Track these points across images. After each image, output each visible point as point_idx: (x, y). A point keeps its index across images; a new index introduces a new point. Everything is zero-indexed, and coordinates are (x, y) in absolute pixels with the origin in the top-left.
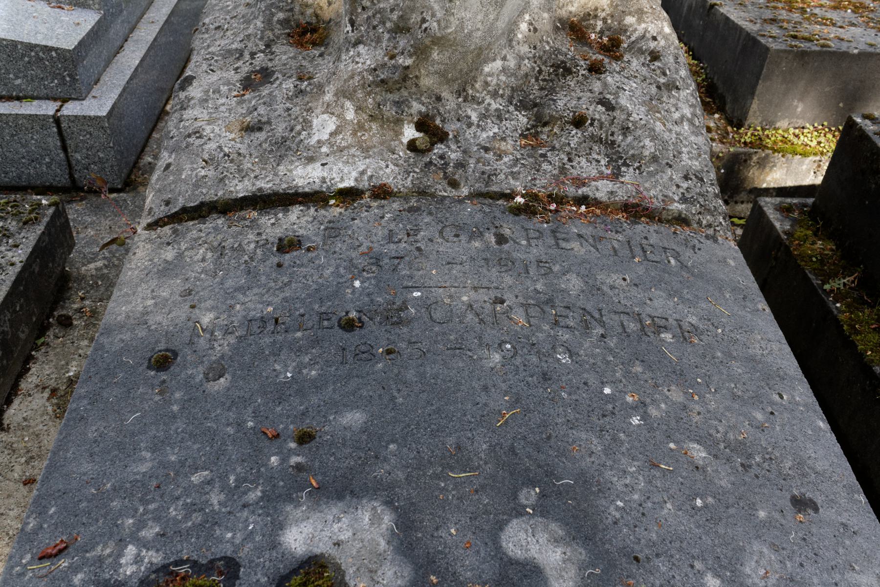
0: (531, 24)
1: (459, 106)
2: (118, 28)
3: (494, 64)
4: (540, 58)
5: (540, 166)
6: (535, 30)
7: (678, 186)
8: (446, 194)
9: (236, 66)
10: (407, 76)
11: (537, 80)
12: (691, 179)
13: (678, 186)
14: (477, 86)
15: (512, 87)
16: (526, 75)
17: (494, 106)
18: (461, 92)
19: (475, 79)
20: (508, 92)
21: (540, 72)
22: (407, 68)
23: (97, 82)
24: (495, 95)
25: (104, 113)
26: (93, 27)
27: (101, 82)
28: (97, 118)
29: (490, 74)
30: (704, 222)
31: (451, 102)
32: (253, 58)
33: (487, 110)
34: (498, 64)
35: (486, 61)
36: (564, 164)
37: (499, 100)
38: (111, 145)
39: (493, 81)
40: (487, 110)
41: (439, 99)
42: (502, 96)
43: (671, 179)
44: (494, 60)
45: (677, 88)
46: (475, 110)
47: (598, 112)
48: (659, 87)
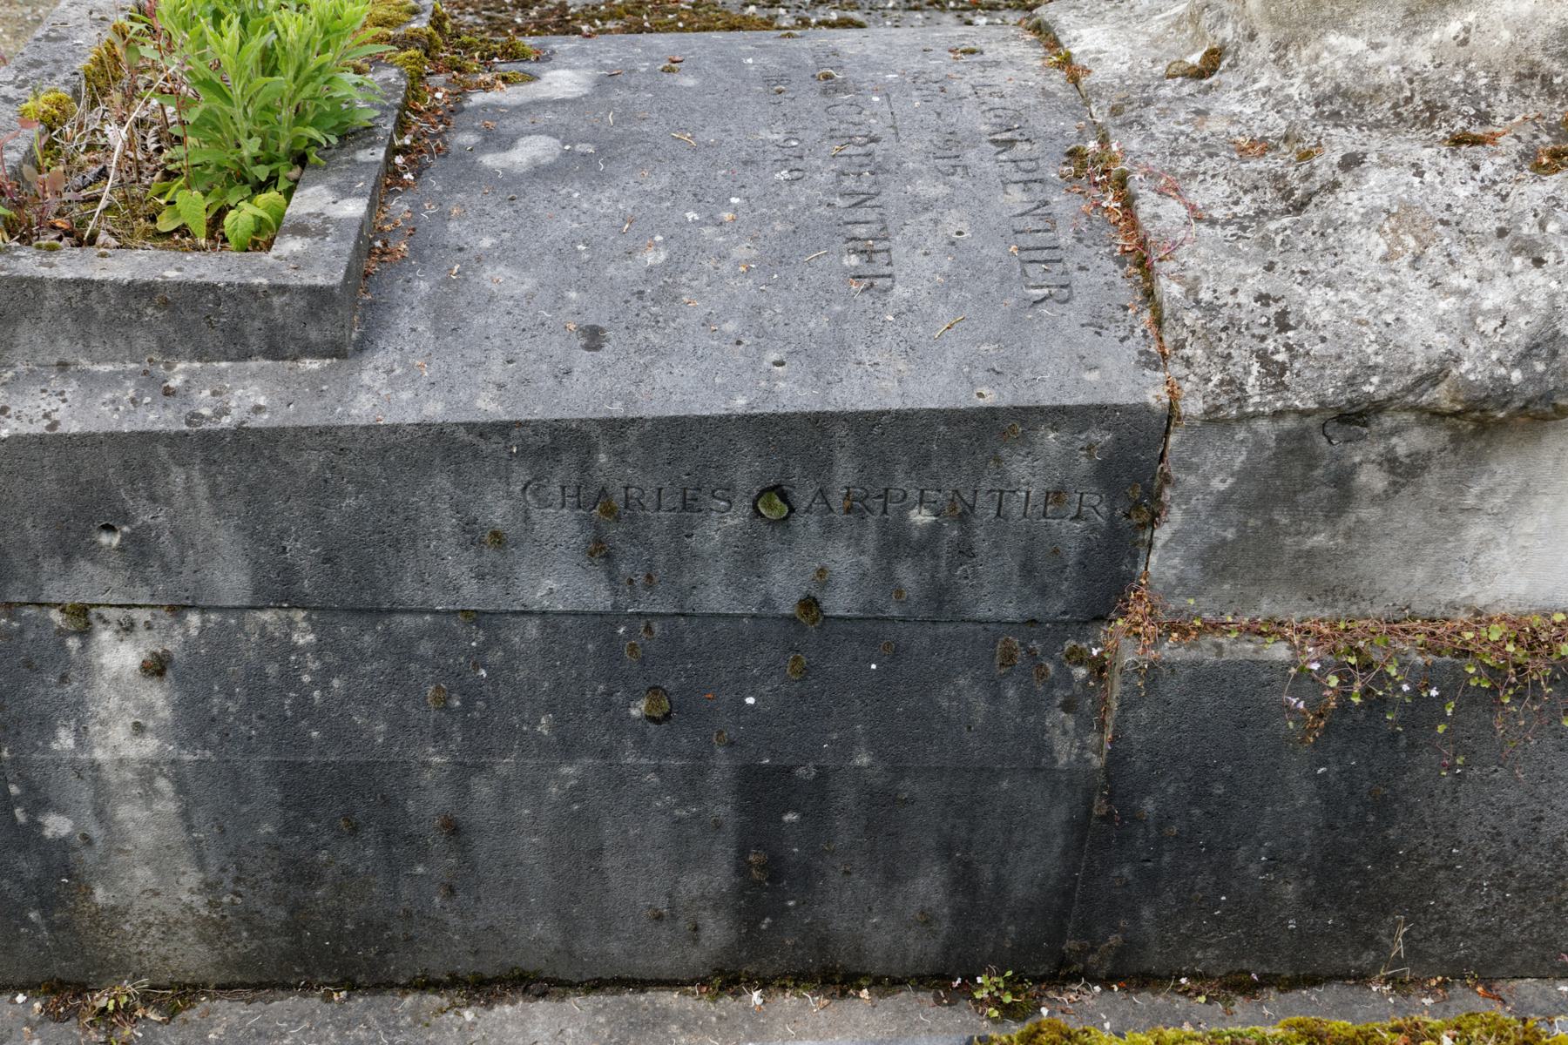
0: (1467, 30)
1: (1264, 62)
3: (1351, 41)
4: (1425, 81)
6: (1465, 42)
7: (1234, 292)
11: (1395, 106)
13: (1234, 292)
14: (1305, 53)
15: (1338, 86)
16: (1379, 88)
17: (1293, 91)
18: (1281, 47)
19: (1306, 41)
20: (1327, 87)
21: (1408, 100)
24: (1309, 77)
29: (1331, 50)
30: (1188, 351)
31: (1261, 50)
33: (1282, 88)
34: (1357, 45)
35: (1339, 25)
37: (1307, 86)
39: (1326, 58)
40: (1282, 88)
41: (1252, 37)
42: (1313, 85)
43: (1242, 278)
44: (1355, 36)
45: (1538, 262)
46: (1272, 78)
48: (1502, 233)
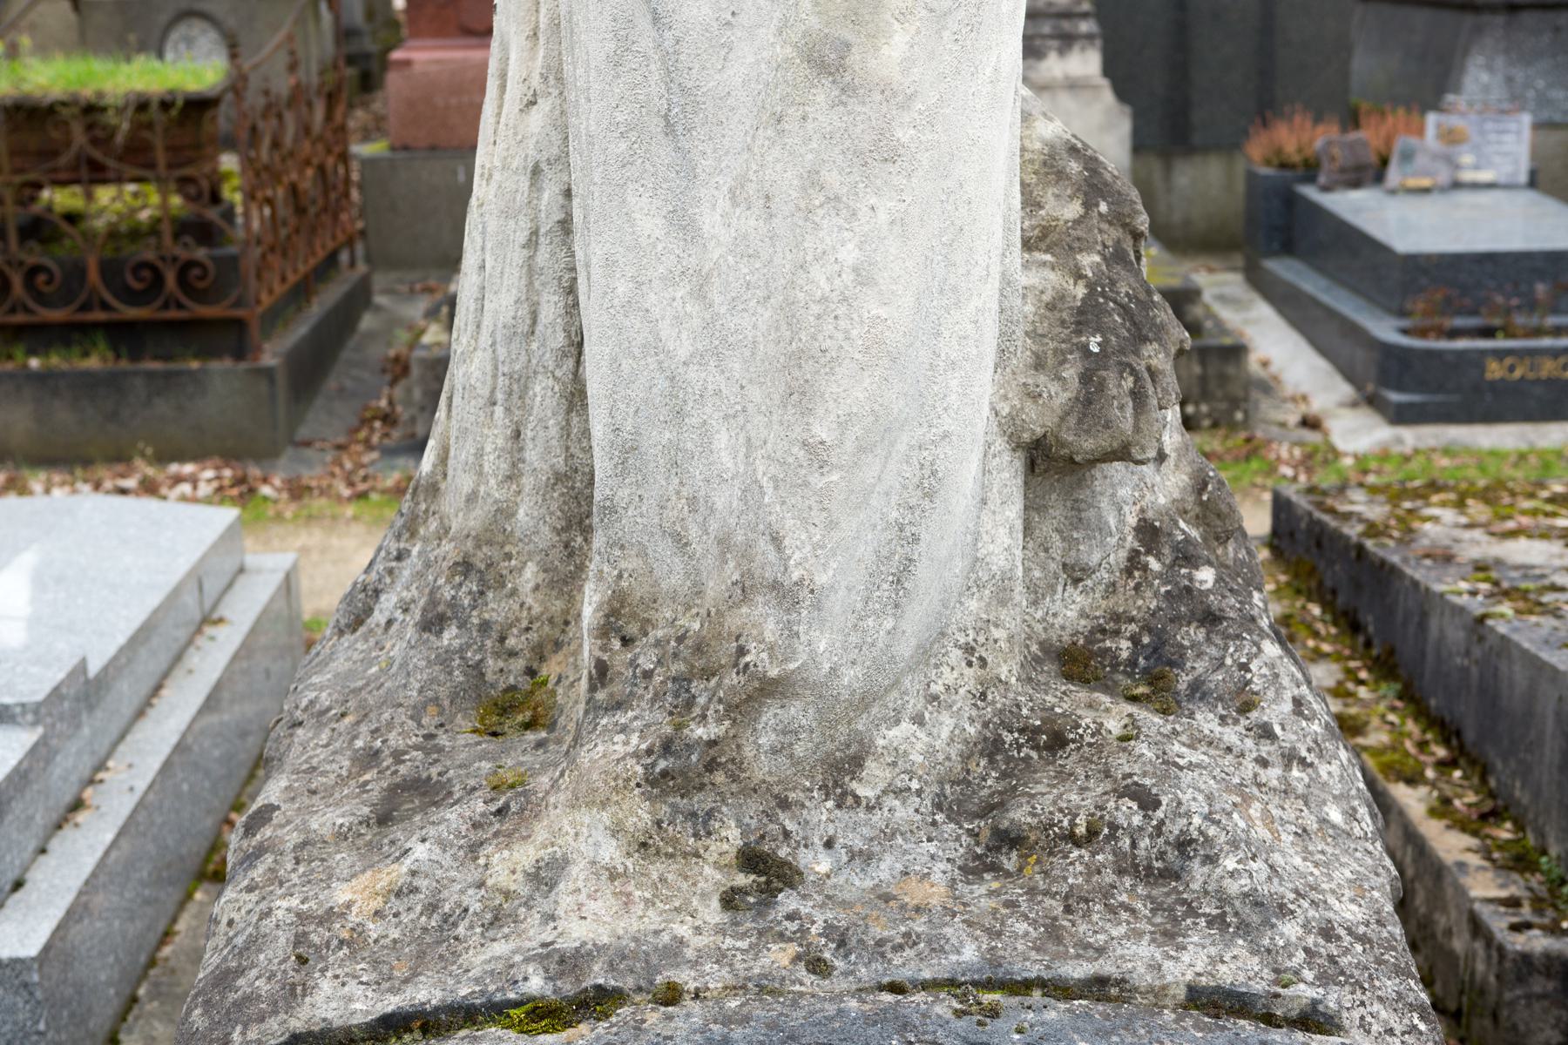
2: (69, 764)
5: (1003, 924)
8: (803, 989)
9: (362, 780)
10: (714, 759)
12: (1339, 938)
22: (712, 743)
23: (18, 885)
25: (31, 949)
26: (20, 763)
27: (27, 886)
28: (15, 962)
32: (399, 762)
36: (1055, 919)
38: (42, 1027)
47: (1127, 813)
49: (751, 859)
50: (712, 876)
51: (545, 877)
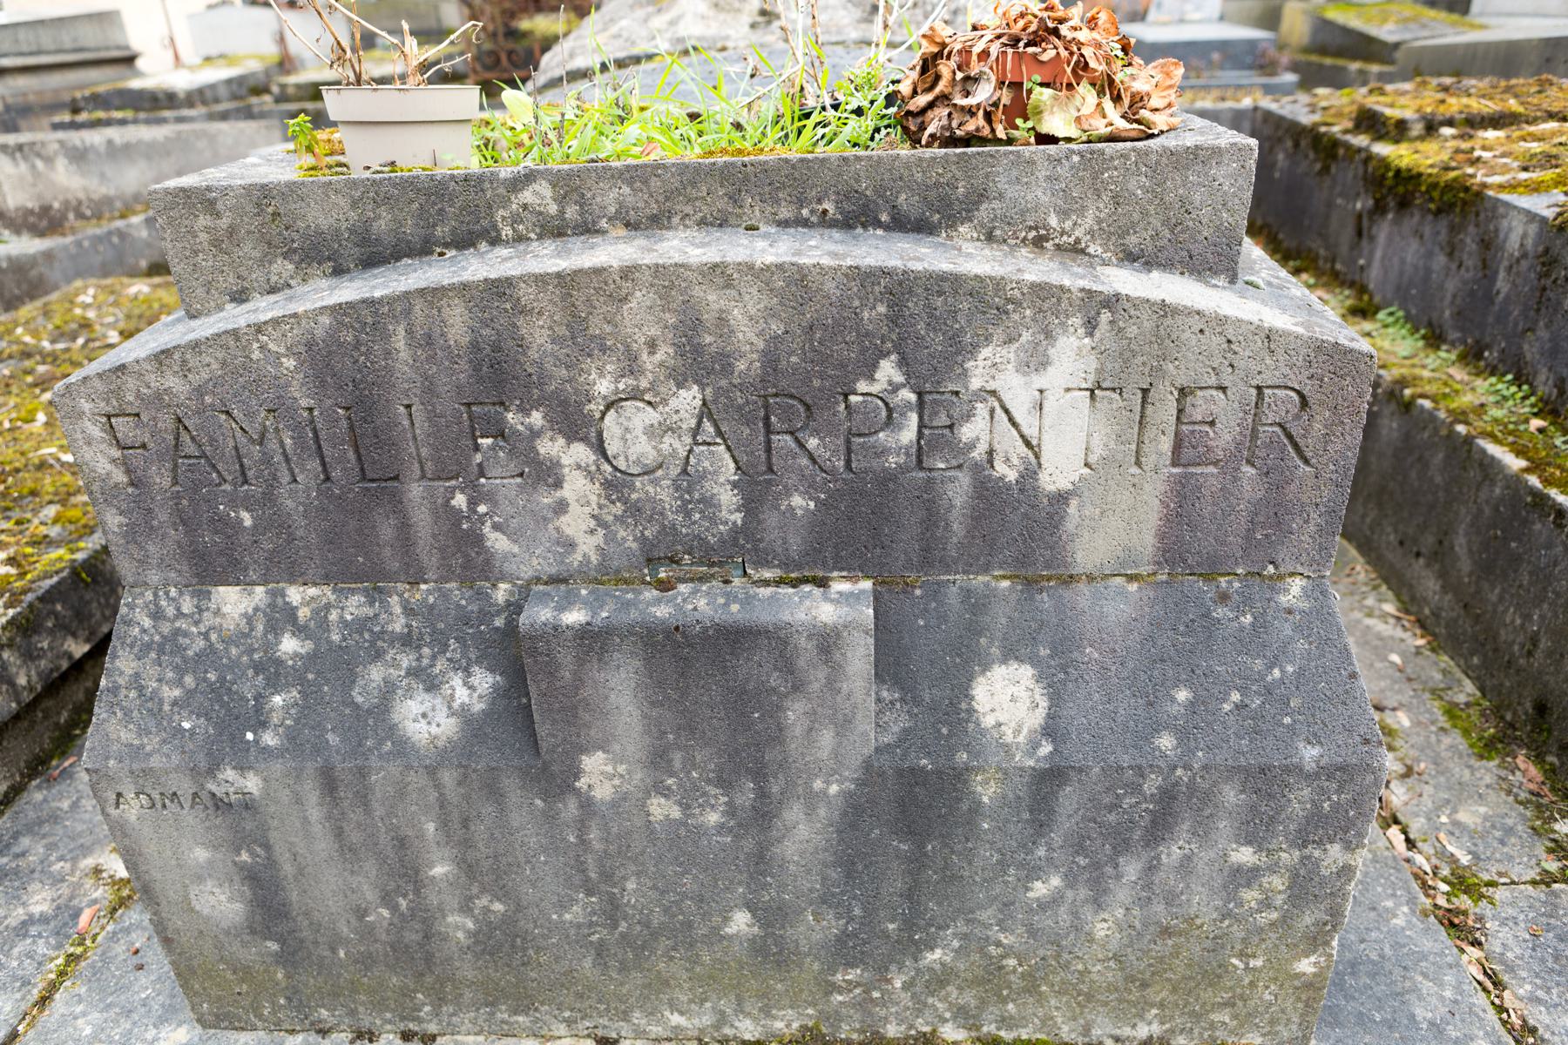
49: (763, 13)
50: (746, 19)
51: (673, 23)
